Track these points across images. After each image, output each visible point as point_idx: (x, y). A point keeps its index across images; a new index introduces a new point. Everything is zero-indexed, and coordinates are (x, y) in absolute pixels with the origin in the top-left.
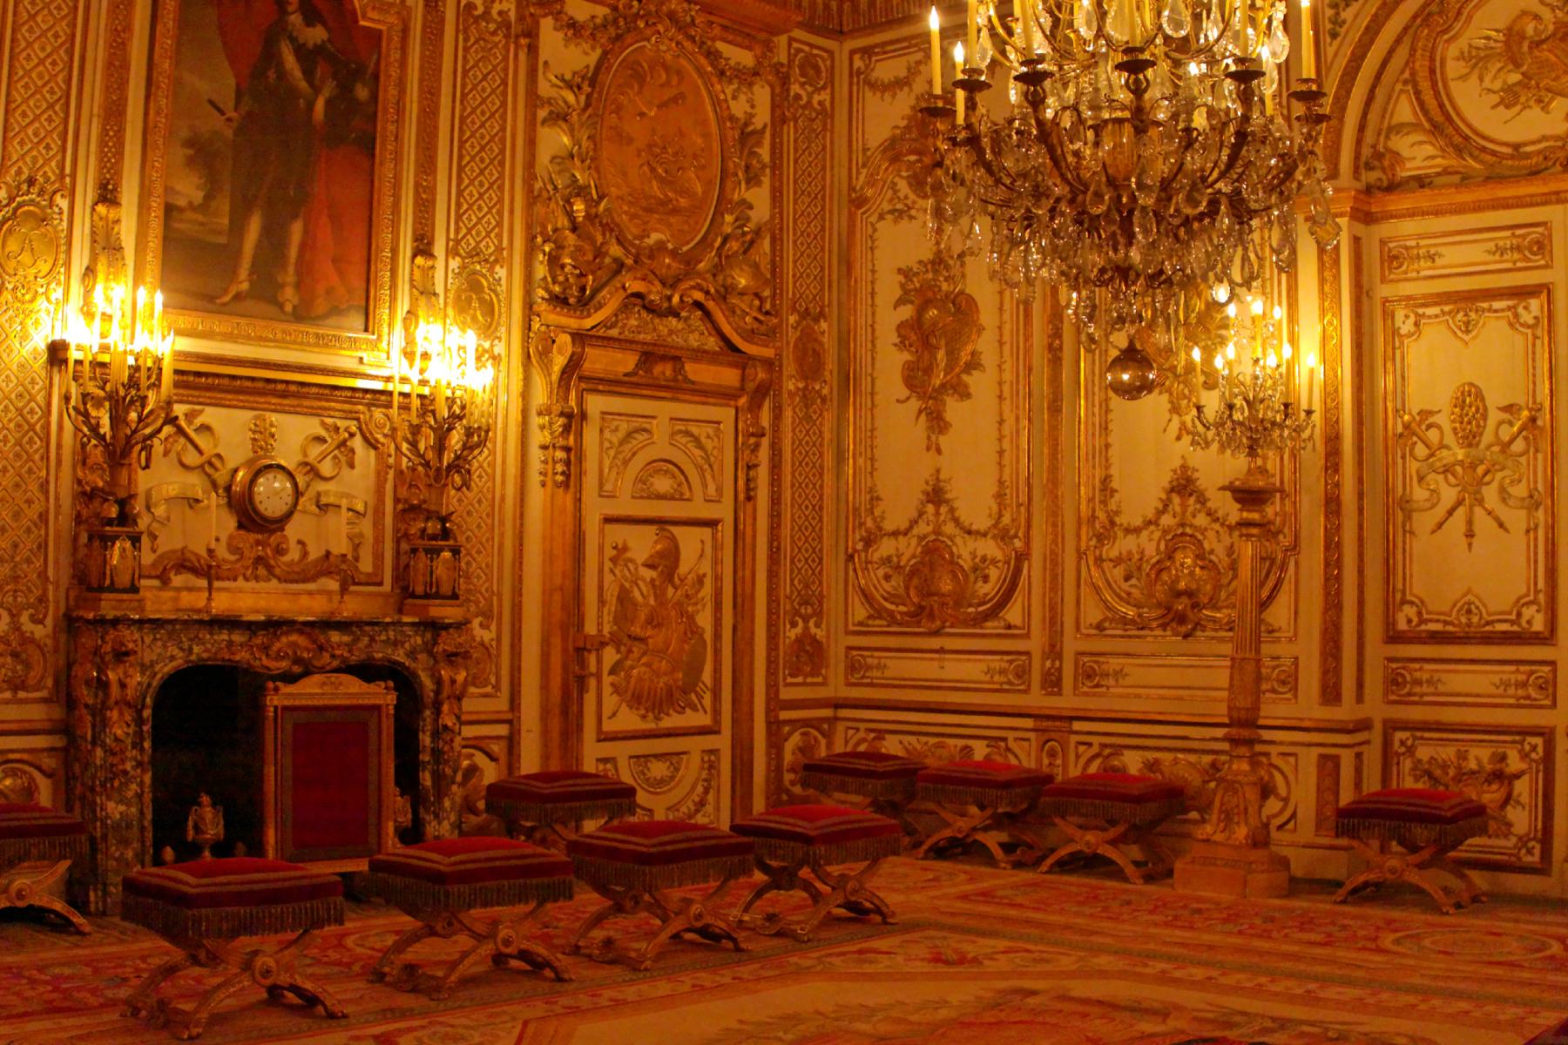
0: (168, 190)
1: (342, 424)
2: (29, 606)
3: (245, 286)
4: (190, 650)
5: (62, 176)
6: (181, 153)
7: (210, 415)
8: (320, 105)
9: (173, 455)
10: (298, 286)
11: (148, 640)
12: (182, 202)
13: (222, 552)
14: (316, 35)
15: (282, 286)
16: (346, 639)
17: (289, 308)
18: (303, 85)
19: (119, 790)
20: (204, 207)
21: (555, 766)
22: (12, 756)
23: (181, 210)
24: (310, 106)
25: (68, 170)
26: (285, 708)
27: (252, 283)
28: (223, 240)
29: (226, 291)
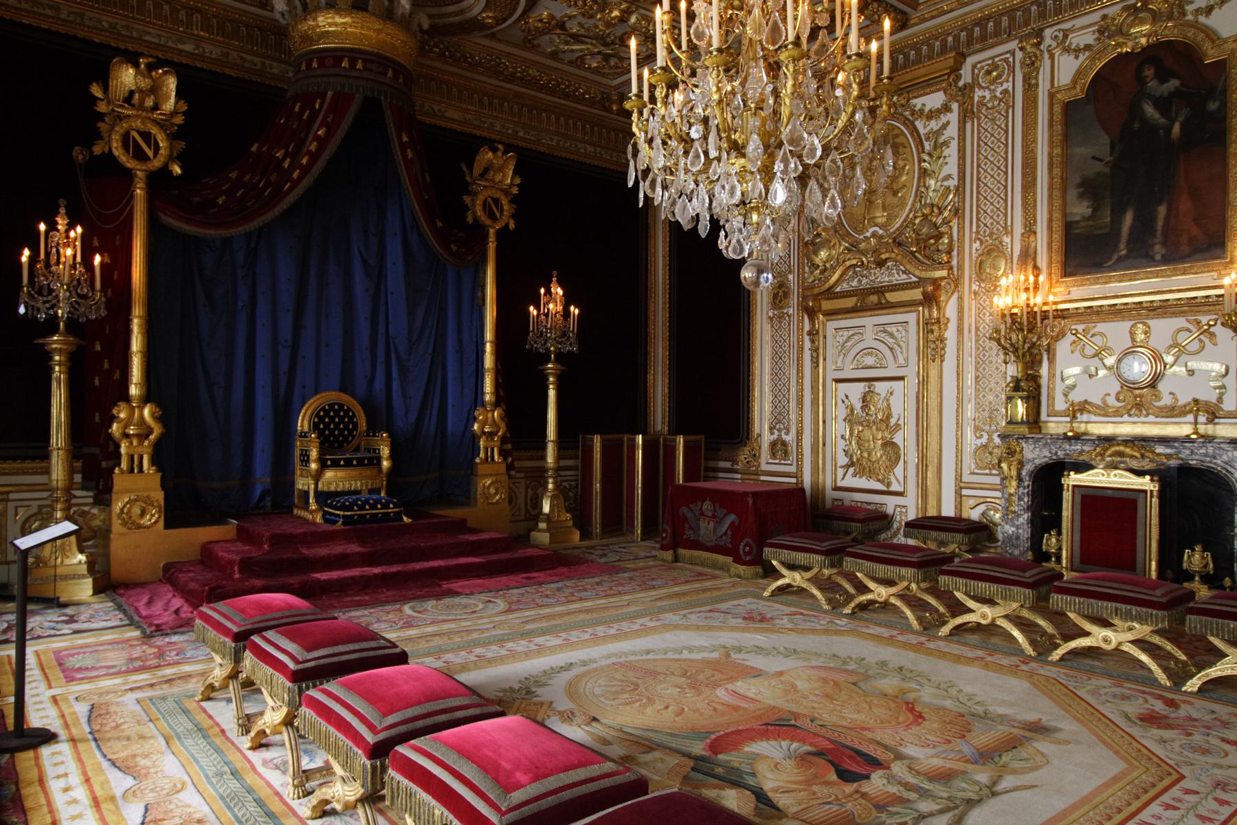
0: (1065, 215)
1: (1204, 319)
2: (997, 430)
3: (1124, 252)
4: (1056, 454)
5: (1006, 228)
6: (1072, 194)
7: (1101, 327)
8: (1176, 128)
9: (1077, 352)
10: (1164, 243)
11: (1031, 447)
12: (1077, 218)
13: (1112, 401)
14: (1174, 83)
15: (1152, 246)
16: (1168, 451)
17: (1158, 257)
18: (1163, 120)
19: (1012, 520)
20: (1093, 217)
21: (958, 515)
22: (989, 500)
23: (1078, 222)
24: (1169, 130)
25: (1009, 223)
26: (1074, 486)
27: (1130, 251)
28: (1107, 230)
29: (1110, 258)
